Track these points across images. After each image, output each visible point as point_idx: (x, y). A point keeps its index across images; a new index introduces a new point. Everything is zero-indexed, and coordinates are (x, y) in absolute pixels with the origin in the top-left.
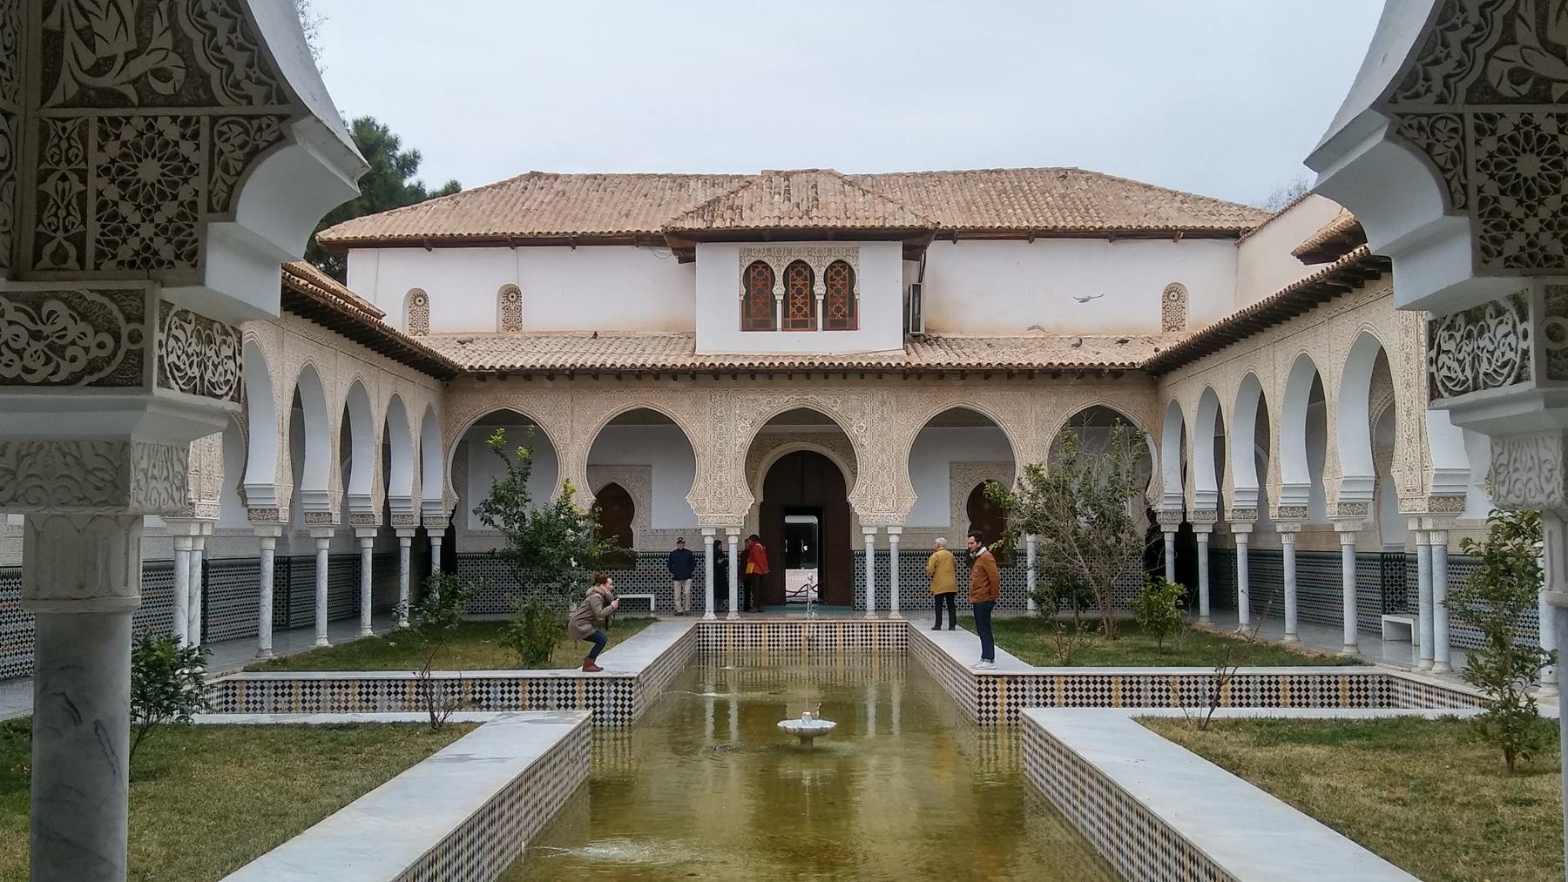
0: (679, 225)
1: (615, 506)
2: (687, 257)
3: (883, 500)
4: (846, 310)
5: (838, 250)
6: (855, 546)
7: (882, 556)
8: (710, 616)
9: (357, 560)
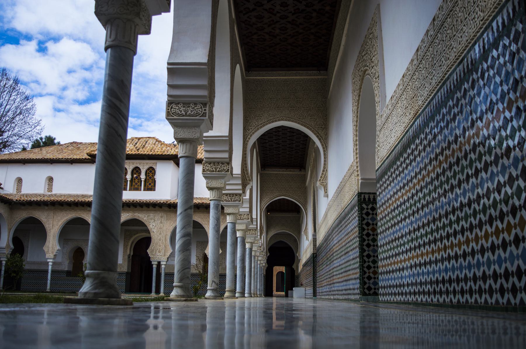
4: (152, 184)
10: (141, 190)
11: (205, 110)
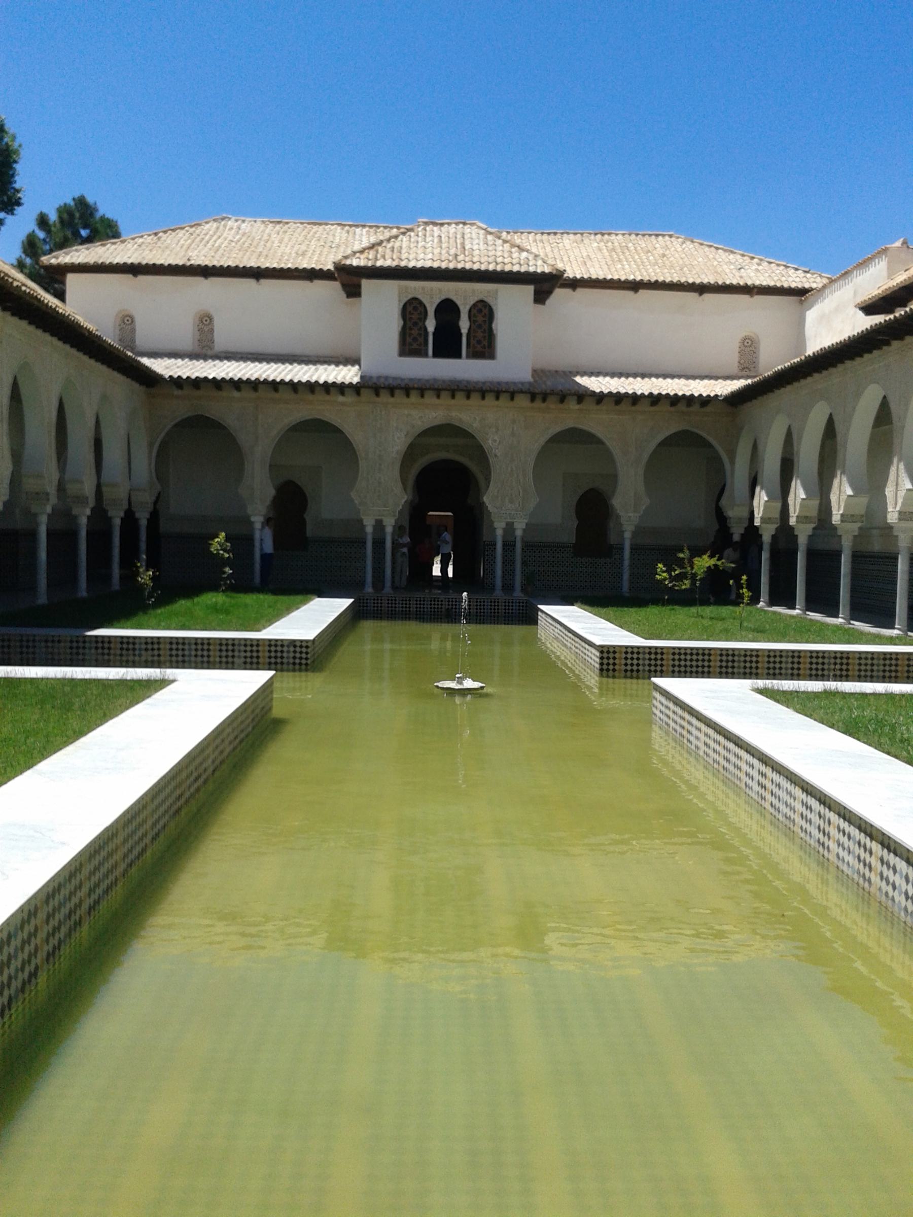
0: (348, 262)
1: (290, 501)
2: (353, 291)
3: (511, 501)
5: (481, 290)
6: (486, 538)
7: (509, 546)
9: (73, 534)
10: (459, 356)
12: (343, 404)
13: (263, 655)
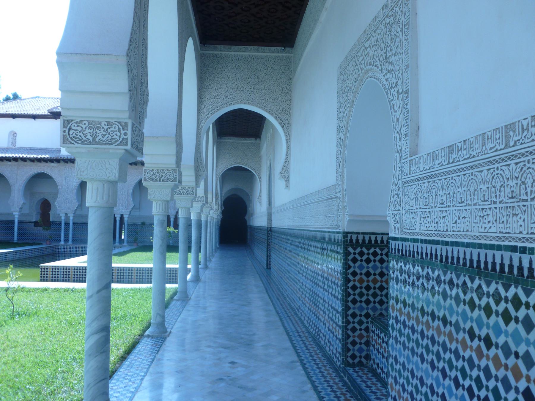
3: (122, 206)
8: (62, 243)
11: (125, 134)
12: (53, 166)
13: (134, 275)
